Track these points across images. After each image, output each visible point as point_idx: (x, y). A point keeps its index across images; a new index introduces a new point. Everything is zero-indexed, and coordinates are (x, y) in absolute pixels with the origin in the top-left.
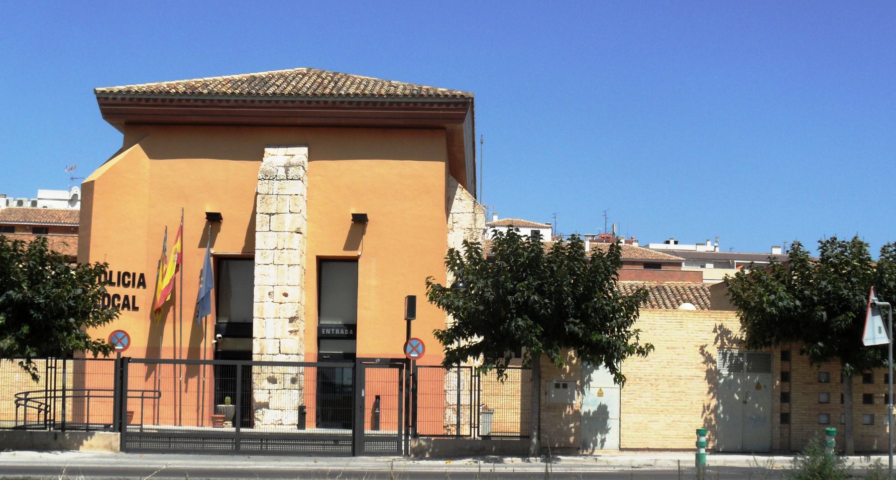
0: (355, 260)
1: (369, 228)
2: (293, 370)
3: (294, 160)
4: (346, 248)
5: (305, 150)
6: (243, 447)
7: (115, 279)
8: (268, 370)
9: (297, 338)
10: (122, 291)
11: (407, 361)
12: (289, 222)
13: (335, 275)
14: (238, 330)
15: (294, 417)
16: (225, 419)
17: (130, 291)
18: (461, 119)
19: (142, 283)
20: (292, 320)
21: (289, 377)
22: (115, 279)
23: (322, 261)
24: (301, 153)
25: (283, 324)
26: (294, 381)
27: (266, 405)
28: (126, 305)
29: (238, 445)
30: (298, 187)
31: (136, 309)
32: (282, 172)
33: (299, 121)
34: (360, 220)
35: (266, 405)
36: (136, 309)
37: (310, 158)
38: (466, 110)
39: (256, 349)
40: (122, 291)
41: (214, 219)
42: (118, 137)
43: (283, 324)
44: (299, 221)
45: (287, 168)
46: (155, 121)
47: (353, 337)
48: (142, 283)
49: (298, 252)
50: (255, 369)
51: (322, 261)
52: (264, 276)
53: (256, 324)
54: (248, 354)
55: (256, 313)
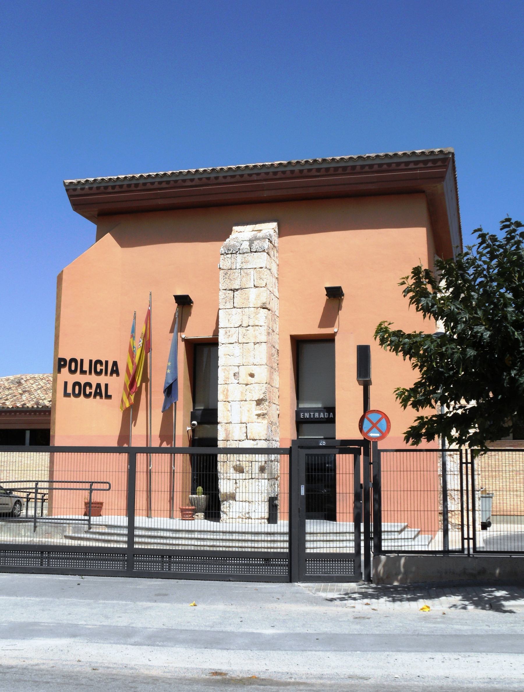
0: (330, 339)
1: (345, 303)
2: (262, 458)
3: (260, 235)
4: (322, 325)
5: (274, 225)
6: (137, 566)
7: (86, 367)
8: (234, 458)
9: (265, 422)
10: (94, 379)
11: (365, 443)
12: (255, 297)
13: (309, 354)
14: (206, 416)
15: (264, 510)
16: (195, 511)
17: (103, 380)
18: (441, 177)
19: (115, 371)
20: (259, 402)
21: (256, 467)
22: (86, 367)
23: (299, 343)
24: (270, 228)
25: (253, 406)
26: (262, 469)
27: (232, 497)
28: (98, 393)
29: (131, 566)
30: (261, 260)
31: (108, 397)
32: (246, 246)
33: (266, 194)
34: (335, 294)
35: (232, 497)
36: (108, 397)
37: (281, 234)
38: (446, 167)
39: (221, 435)
40: (94, 379)
41: (184, 302)
42: (92, 227)
43: (253, 406)
44: (263, 296)
45: (251, 242)
46: (125, 209)
47: (332, 421)
48: (115, 371)
49: (263, 330)
50: (221, 457)
51: (299, 343)
52: (227, 357)
53: (221, 407)
54: (214, 442)
55: (220, 397)
